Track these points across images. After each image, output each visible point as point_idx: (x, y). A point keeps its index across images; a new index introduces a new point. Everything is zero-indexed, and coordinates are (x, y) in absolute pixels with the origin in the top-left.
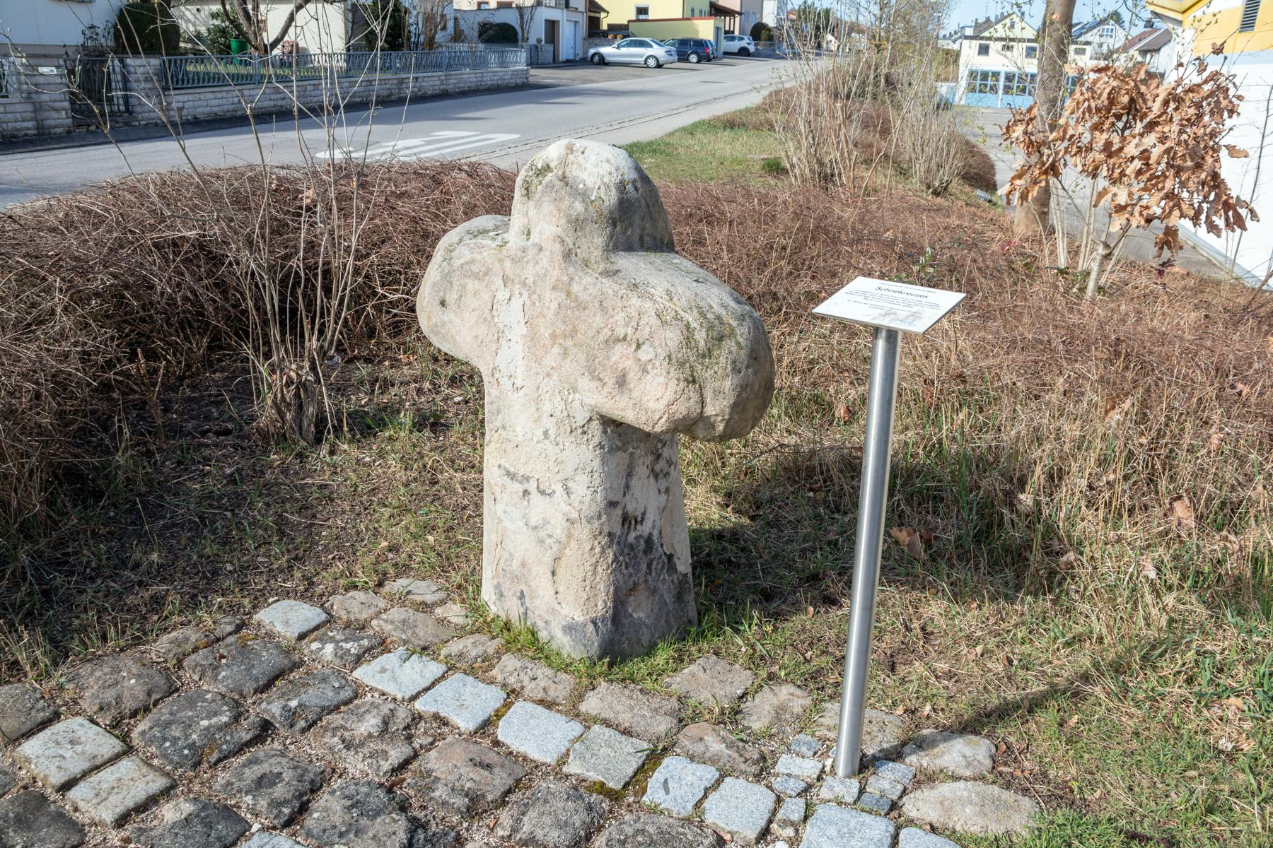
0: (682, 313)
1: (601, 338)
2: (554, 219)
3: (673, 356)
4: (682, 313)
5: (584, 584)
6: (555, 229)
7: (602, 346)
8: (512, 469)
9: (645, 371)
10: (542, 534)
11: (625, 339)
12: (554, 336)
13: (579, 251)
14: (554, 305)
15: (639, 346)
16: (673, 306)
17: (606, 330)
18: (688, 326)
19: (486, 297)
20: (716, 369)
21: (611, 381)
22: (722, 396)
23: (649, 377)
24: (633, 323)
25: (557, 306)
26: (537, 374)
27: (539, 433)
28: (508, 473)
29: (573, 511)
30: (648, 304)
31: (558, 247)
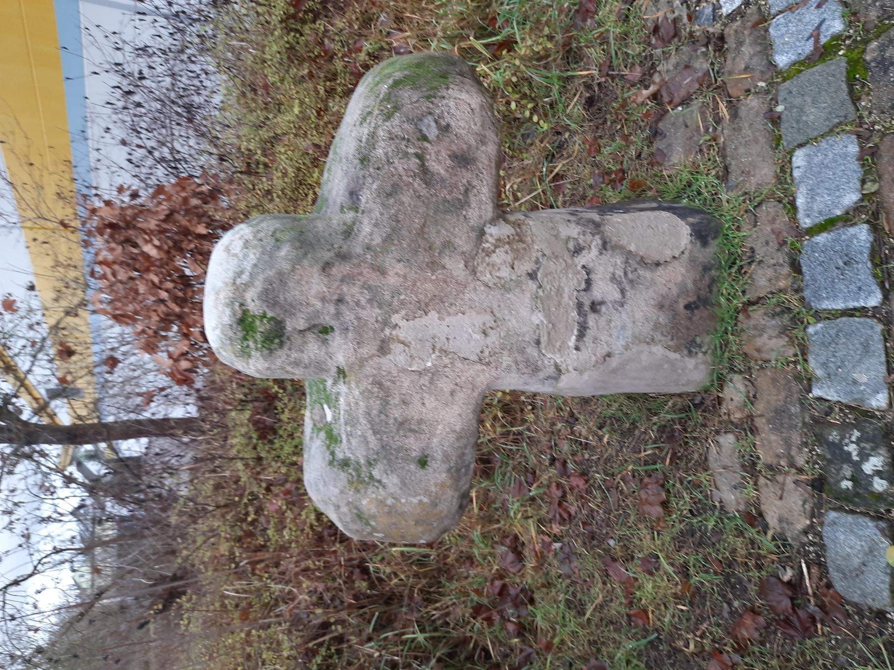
1: (423, 192)
3: (426, 94)
12: (433, 265)
17: (416, 185)
21: (465, 176)
23: (453, 124)
28: (581, 335)
29: (594, 243)
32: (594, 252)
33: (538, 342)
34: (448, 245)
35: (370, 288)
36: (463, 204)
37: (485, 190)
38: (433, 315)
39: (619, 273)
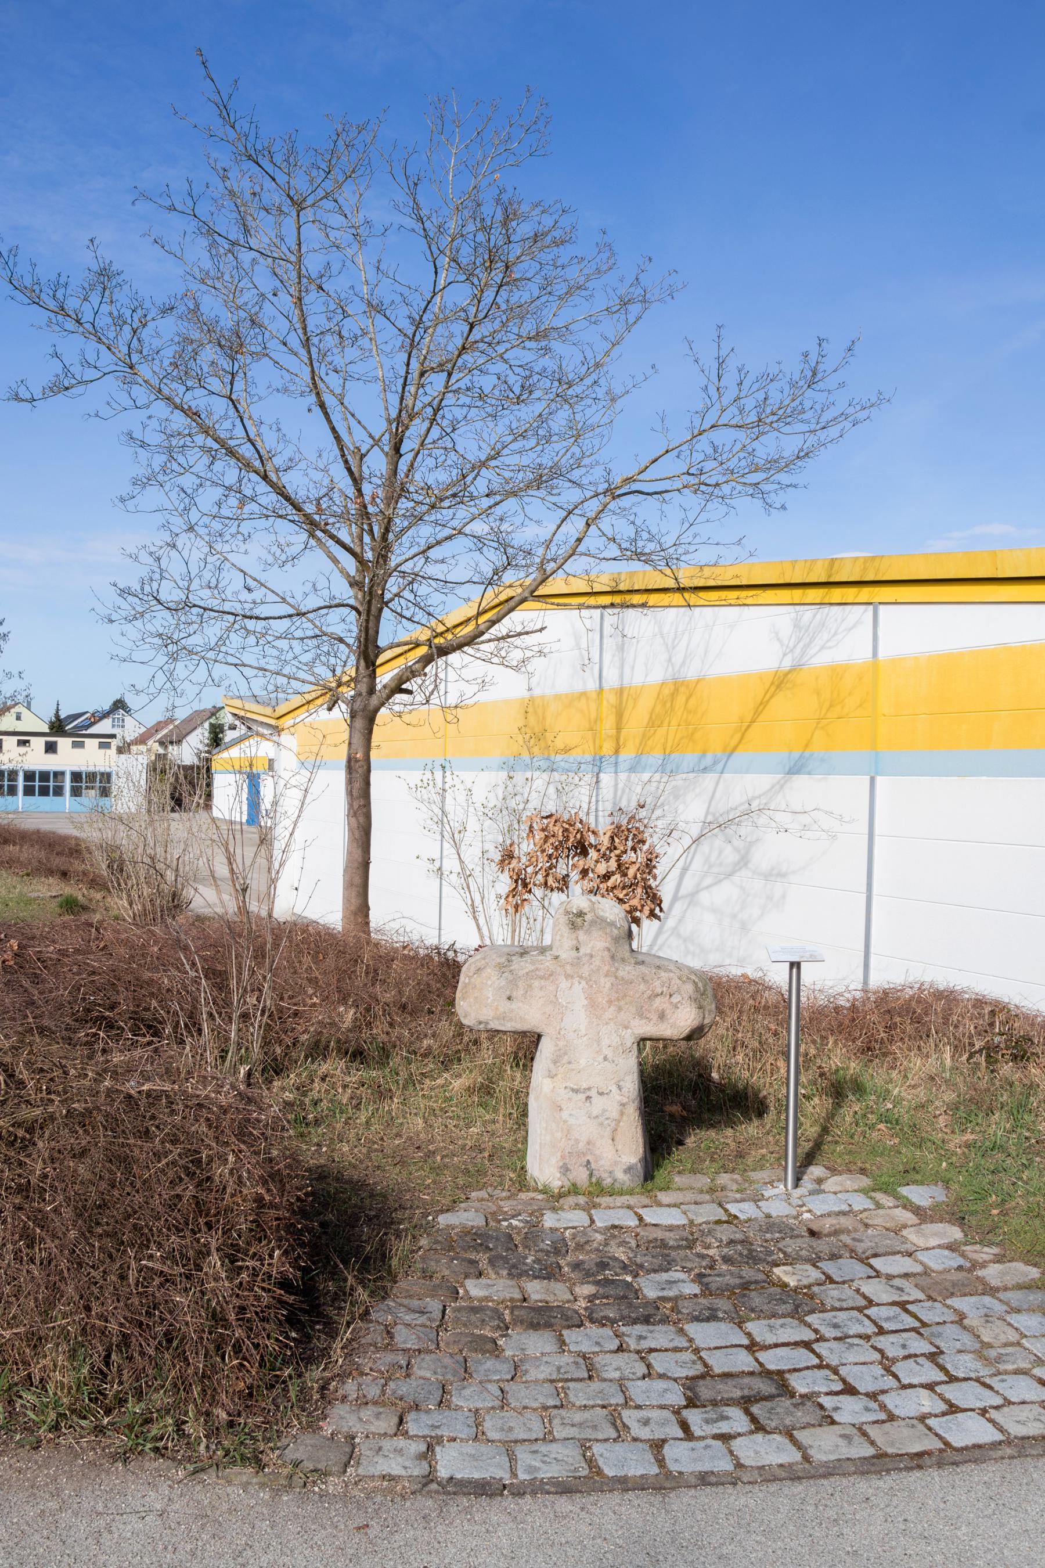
1: (645, 996)
10: (601, 1119)
12: (610, 1002)
14: (608, 985)
15: (671, 996)
21: (654, 1017)
27: (601, 1058)
28: (573, 1090)
30: (672, 974)
31: (606, 953)
32: (619, 1098)
33: (570, 1063)
34: (620, 1009)
35: (598, 970)
36: (641, 1016)
37: (648, 1028)
38: (586, 1002)
39: (607, 1114)
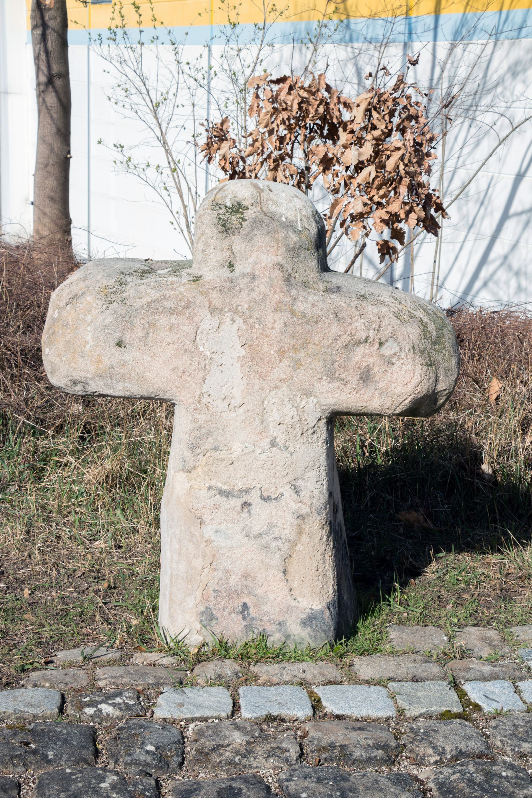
0: (413, 312)
1: (340, 344)
2: (272, 250)
3: (416, 346)
4: (413, 312)
5: (317, 573)
6: (274, 258)
7: (340, 351)
8: (225, 487)
9: (391, 363)
10: (267, 539)
11: (366, 340)
12: (282, 353)
13: (297, 275)
14: (279, 325)
15: (381, 344)
16: (405, 308)
17: (345, 337)
18: (421, 321)
19: (188, 329)
20: (444, 352)
21: (354, 379)
22: (450, 373)
23: (394, 368)
24: (374, 326)
25: (282, 325)
26: (262, 389)
27: (266, 443)
28: (221, 492)
29: (303, 507)
30: (384, 309)
31: (277, 273)
32: (295, 506)
33: (216, 449)
34: (298, 364)
35: (264, 300)
36: (332, 376)
37: (344, 396)
38: (242, 352)
39: (276, 532)
